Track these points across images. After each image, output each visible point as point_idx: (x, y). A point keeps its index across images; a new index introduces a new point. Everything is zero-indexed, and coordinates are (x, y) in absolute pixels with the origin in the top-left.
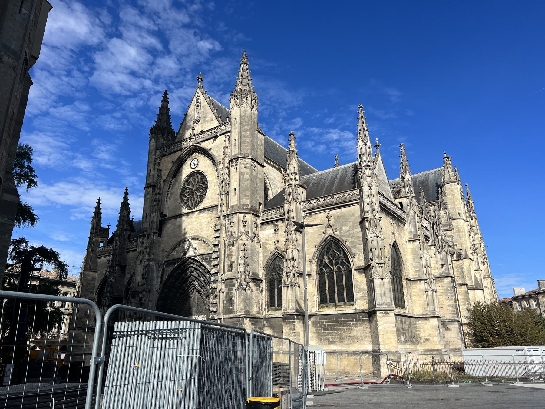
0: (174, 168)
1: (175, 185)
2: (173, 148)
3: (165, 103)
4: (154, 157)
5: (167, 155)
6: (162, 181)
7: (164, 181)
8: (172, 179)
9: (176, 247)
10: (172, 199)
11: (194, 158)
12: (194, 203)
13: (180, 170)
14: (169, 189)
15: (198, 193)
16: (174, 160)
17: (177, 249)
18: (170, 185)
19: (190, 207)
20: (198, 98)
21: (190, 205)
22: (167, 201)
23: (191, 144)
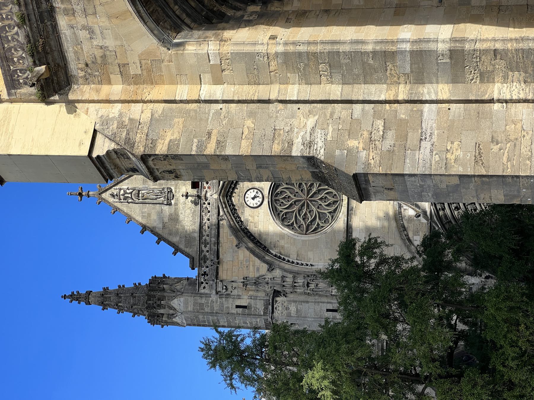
0: (251, 245)
1: (283, 247)
2: (207, 249)
3: (91, 299)
4: (214, 297)
5: (218, 263)
6: (269, 276)
7: (271, 268)
8: (270, 253)
9: (407, 235)
10: (310, 255)
11: (242, 200)
12: (332, 200)
13: (256, 236)
14: (288, 261)
15: (314, 190)
16: (235, 242)
17: (411, 235)
18: (280, 258)
19: (335, 210)
20: (122, 192)
21: (332, 209)
22: (312, 265)
23: (216, 196)
